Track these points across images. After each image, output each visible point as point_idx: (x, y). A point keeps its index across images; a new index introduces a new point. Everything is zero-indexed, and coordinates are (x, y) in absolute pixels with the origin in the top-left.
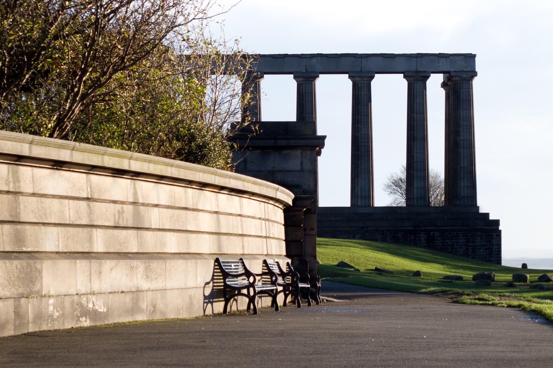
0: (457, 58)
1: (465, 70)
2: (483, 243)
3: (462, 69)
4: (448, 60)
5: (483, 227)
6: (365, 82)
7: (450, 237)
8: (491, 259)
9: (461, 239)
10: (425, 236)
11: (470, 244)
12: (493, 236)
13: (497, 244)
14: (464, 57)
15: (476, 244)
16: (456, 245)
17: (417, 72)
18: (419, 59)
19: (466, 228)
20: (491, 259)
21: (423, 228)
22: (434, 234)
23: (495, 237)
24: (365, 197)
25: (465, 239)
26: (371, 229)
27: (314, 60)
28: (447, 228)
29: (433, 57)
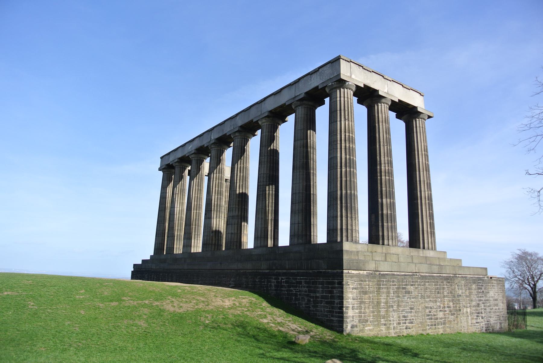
0: (325, 68)
1: (331, 77)
2: (324, 294)
3: (329, 78)
4: (318, 73)
5: (327, 270)
6: (265, 124)
7: (294, 283)
8: (332, 318)
9: (304, 287)
10: (275, 281)
11: (312, 294)
12: (334, 283)
13: (339, 296)
14: (330, 64)
15: (318, 295)
16: (300, 295)
17: (295, 97)
18: (297, 84)
19: (311, 271)
20: (332, 318)
21: (276, 271)
22: (282, 279)
23: (337, 286)
24: (258, 238)
25: (307, 287)
26: (242, 271)
27: (238, 117)
28: (295, 271)
29: (307, 77)
